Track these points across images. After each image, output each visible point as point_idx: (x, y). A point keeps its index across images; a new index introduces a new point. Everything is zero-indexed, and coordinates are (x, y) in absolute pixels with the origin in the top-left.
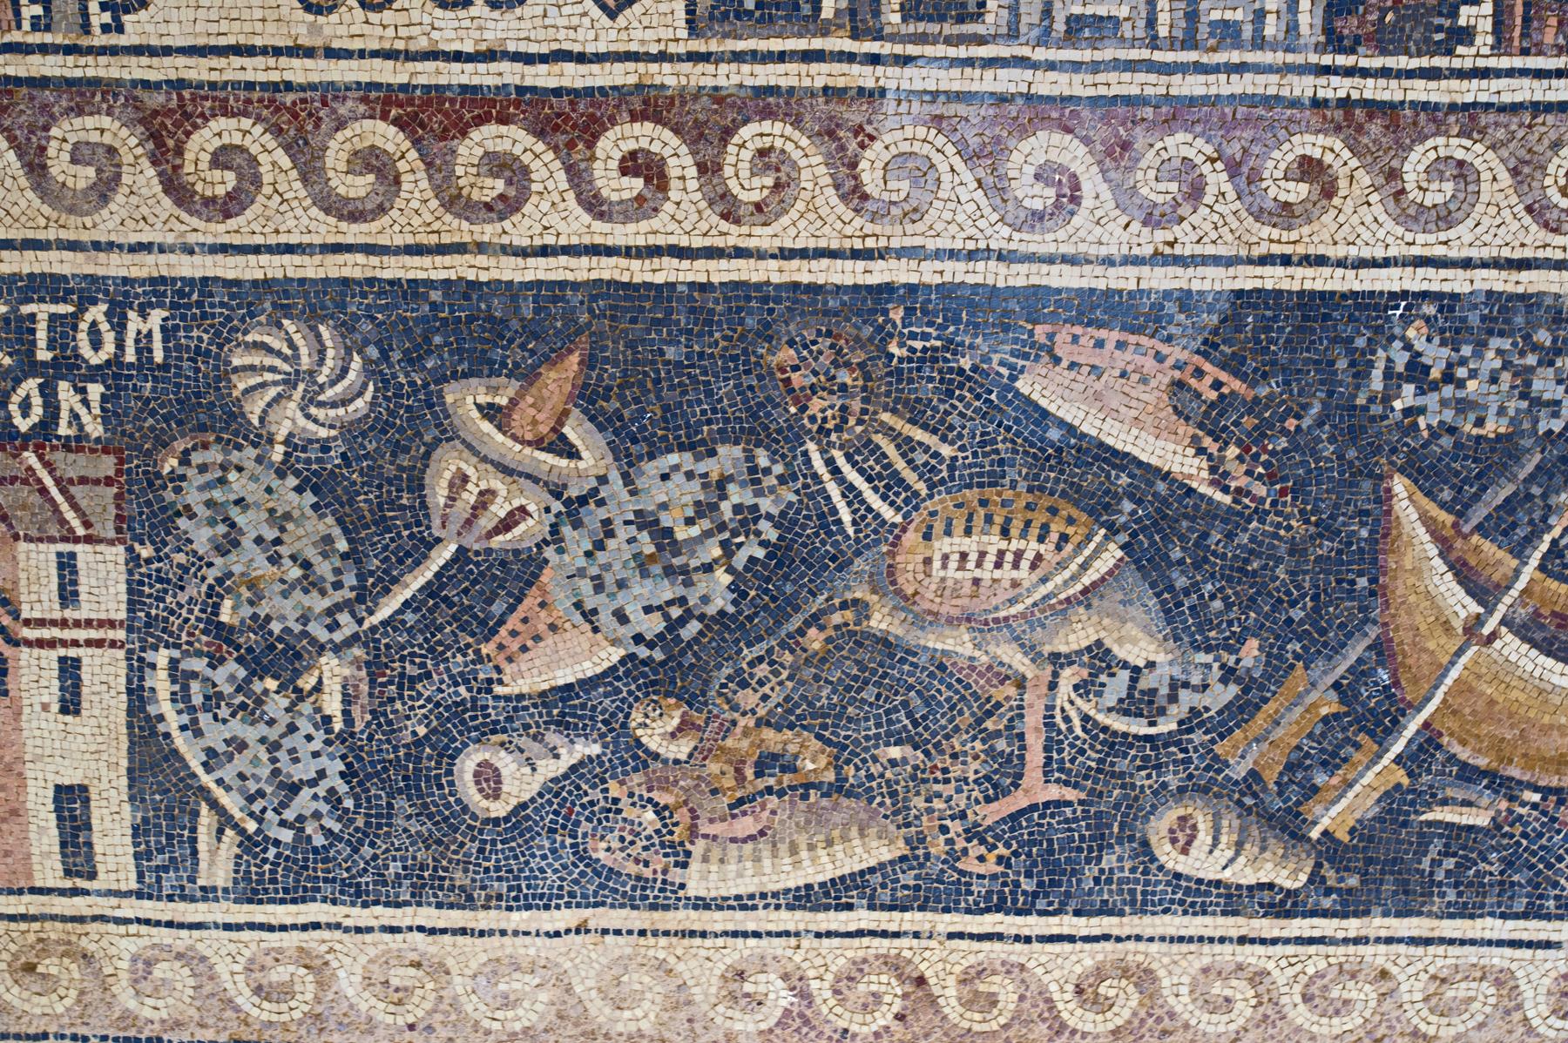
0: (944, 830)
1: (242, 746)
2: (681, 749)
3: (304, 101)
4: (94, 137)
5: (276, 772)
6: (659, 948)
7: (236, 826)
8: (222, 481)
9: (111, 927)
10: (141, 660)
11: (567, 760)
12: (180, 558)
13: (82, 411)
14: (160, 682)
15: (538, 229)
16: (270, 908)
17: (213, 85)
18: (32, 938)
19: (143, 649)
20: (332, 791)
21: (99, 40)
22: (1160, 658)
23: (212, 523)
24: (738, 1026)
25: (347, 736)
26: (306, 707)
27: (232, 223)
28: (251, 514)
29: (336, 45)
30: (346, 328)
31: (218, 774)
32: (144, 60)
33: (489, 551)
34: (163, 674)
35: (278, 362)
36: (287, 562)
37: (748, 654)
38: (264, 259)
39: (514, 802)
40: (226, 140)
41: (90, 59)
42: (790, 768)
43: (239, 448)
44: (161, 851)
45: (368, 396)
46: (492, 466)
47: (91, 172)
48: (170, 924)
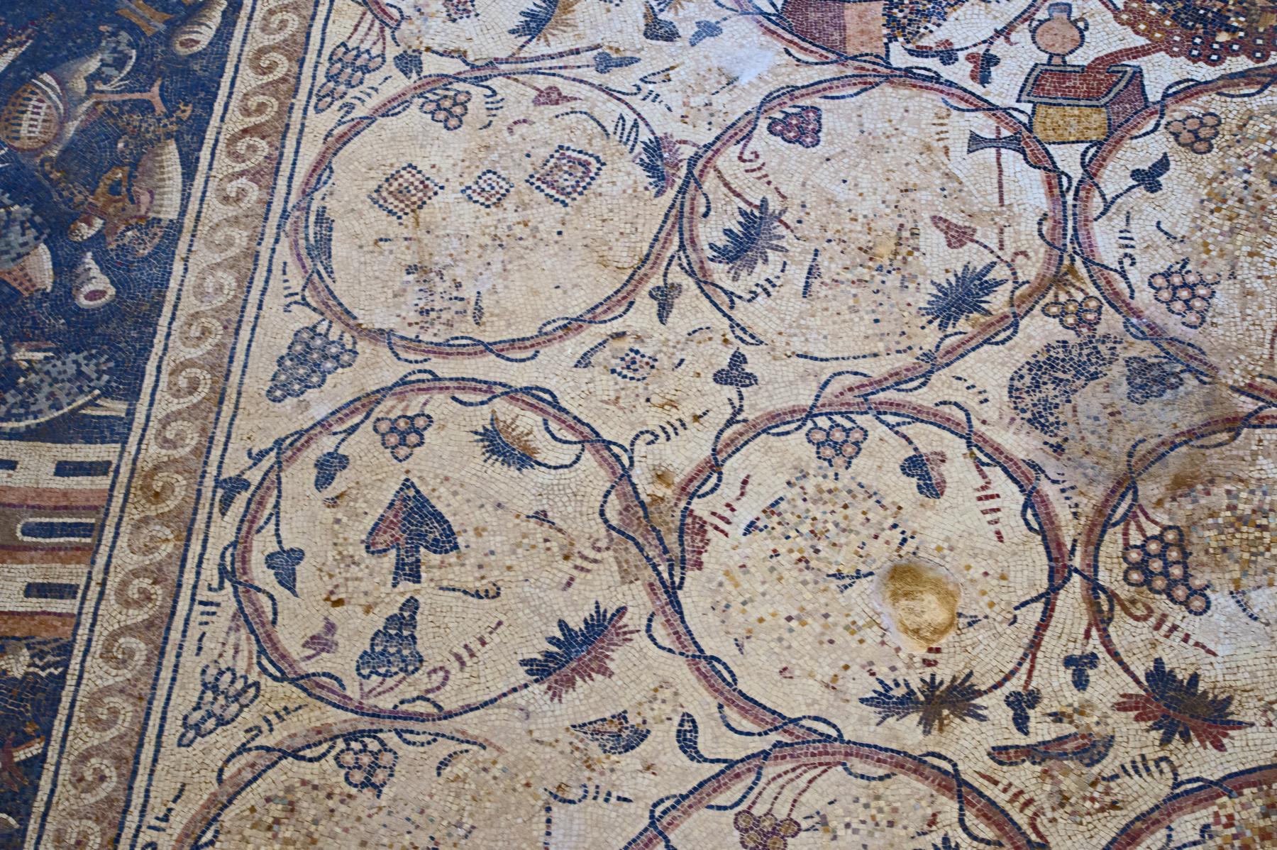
0: (165, 126)
1: (52, 394)
2: (98, 223)
5: (69, 381)
6: (203, 229)
7: (95, 399)
9: (140, 456)
11: (93, 265)
18: (139, 493)
20: (85, 358)
22: (99, 57)
24: (254, 198)
25: (57, 351)
26: (37, 366)
37: (56, 198)
42: (119, 183)
44: (102, 432)
48: (144, 430)
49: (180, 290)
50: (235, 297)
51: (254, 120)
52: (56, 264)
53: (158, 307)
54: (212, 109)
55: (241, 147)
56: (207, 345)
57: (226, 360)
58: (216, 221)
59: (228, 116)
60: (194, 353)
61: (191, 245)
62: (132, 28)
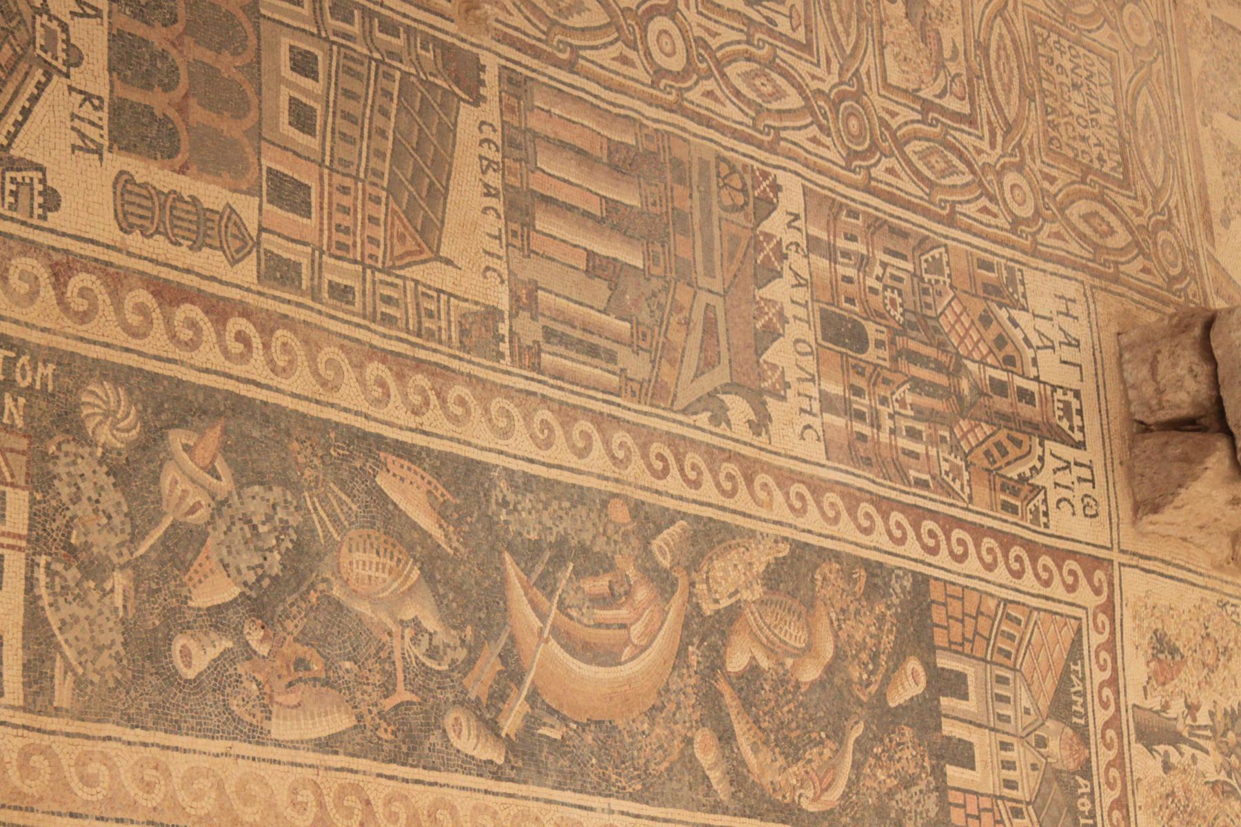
0: (370, 712)
1: (77, 621)
4: (29, 269)
5: (93, 638)
7: (72, 670)
8: (74, 463)
9: (9, 730)
10: (33, 560)
11: (219, 650)
12: (54, 503)
13: (14, 411)
14: (41, 574)
15: (204, 359)
16: (89, 725)
17: (81, 256)
19: (34, 554)
20: (117, 653)
21: (36, 222)
22: (438, 629)
23: (69, 485)
26: (107, 600)
27: (84, 327)
28: (86, 483)
29: (131, 250)
30: (129, 392)
31: (66, 636)
32: (54, 236)
33: (185, 523)
34: (42, 570)
35: (100, 403)
36: (101, 513)
37: (290, 600)
38: (98, 348)
39: (198, 671)
42: (307, 669)
43: (82, 446)
45: (138, 429)
46: (190, 476)
47: (27, 286)
48: (39, 730)
49: (195, 751)
50: (189, 816)
51: (379, 808)
52: (220, 608)
53: (176, 728)
54: (390, 761)
55: (351, 800)
56: (133, 790)
57: (119, 815)
58: (271, 783)
59: (383, 781)
60: (126, 778)
61: (243, 757)
62: (470, 662)
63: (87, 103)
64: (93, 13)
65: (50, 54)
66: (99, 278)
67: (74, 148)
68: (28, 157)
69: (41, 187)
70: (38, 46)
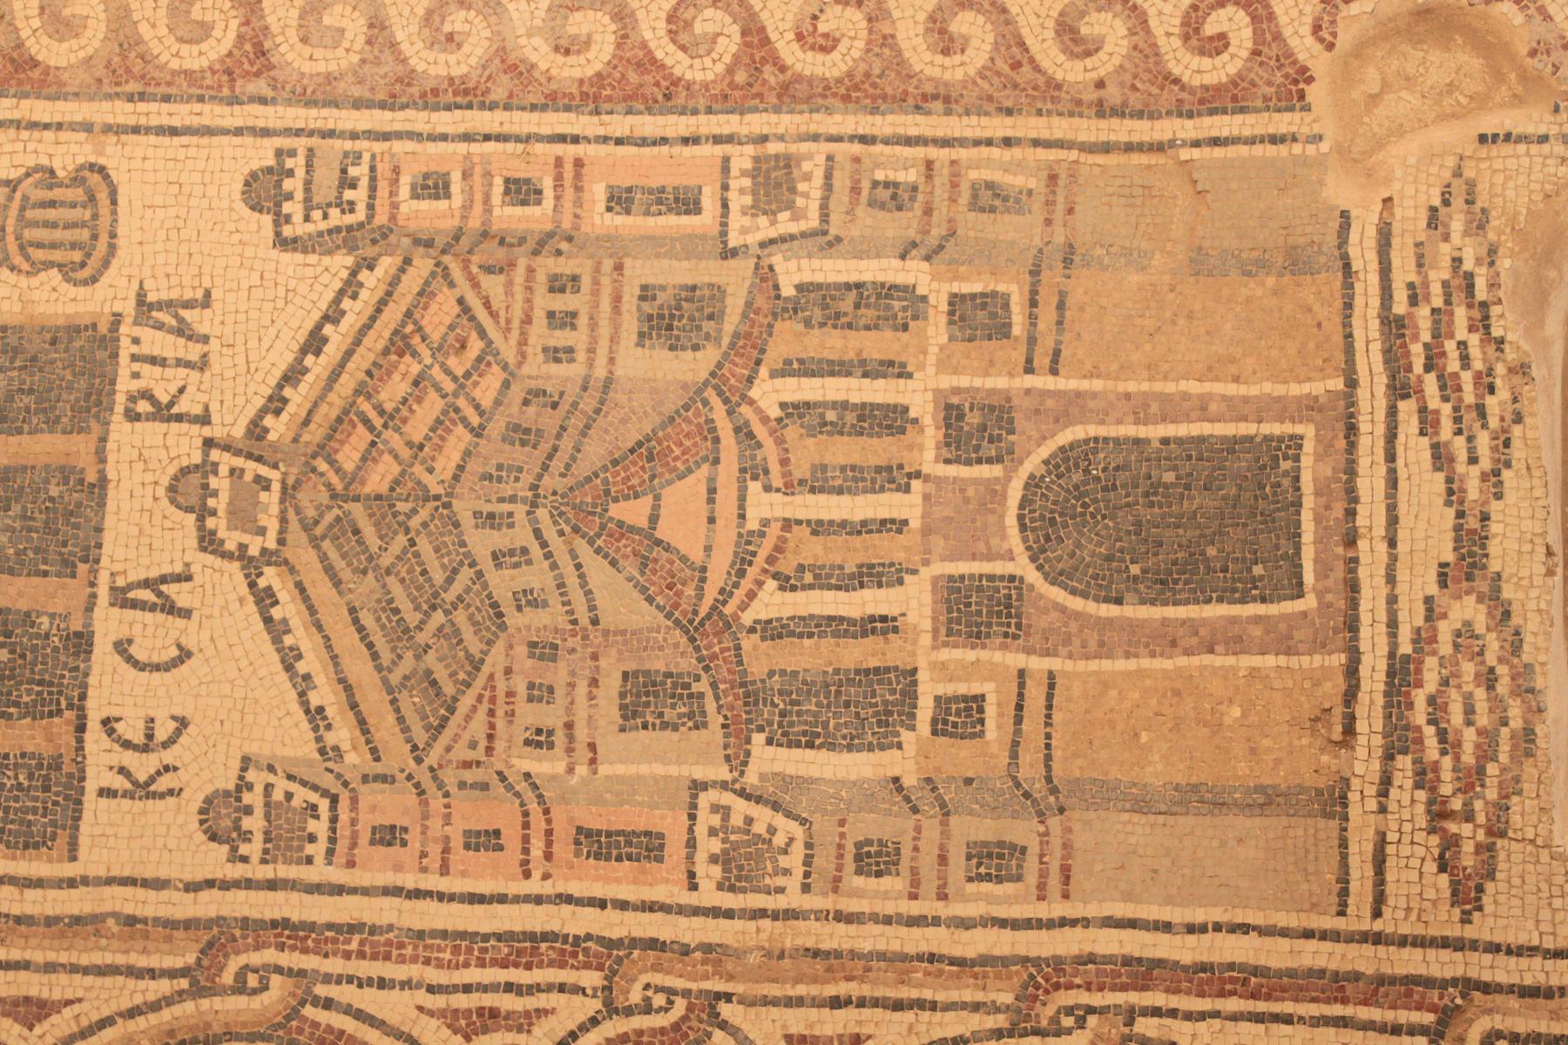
3: (118, 84)
4: (319, 53)
17: (201, 99)
21: (301, 144)
29: (82, 136)
32: (261, 123)
40: (195, 49)
41: (312, 125)
47: (327, 20)
63: (164, 399)
64: (131, 595)
65: (248, 477)
66: (162, 68)
67: (206, 301)
68: (312, 258)
69: (287, 208)
70: (276, 486)
